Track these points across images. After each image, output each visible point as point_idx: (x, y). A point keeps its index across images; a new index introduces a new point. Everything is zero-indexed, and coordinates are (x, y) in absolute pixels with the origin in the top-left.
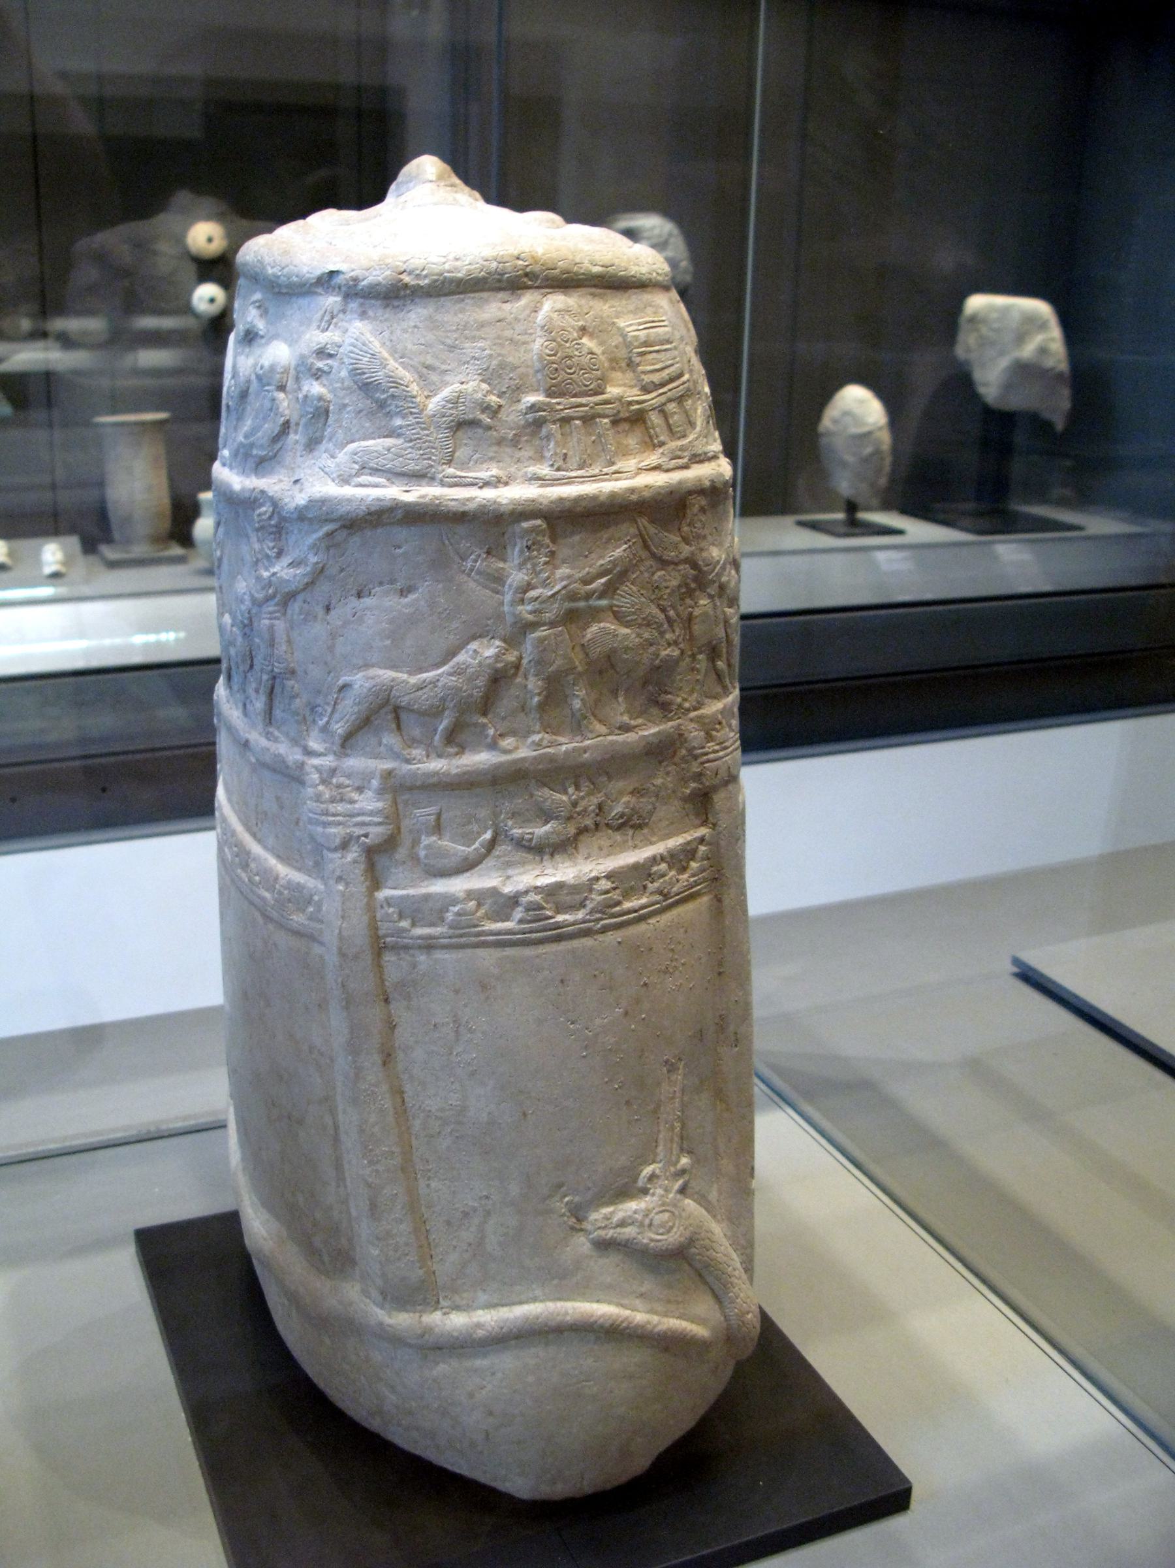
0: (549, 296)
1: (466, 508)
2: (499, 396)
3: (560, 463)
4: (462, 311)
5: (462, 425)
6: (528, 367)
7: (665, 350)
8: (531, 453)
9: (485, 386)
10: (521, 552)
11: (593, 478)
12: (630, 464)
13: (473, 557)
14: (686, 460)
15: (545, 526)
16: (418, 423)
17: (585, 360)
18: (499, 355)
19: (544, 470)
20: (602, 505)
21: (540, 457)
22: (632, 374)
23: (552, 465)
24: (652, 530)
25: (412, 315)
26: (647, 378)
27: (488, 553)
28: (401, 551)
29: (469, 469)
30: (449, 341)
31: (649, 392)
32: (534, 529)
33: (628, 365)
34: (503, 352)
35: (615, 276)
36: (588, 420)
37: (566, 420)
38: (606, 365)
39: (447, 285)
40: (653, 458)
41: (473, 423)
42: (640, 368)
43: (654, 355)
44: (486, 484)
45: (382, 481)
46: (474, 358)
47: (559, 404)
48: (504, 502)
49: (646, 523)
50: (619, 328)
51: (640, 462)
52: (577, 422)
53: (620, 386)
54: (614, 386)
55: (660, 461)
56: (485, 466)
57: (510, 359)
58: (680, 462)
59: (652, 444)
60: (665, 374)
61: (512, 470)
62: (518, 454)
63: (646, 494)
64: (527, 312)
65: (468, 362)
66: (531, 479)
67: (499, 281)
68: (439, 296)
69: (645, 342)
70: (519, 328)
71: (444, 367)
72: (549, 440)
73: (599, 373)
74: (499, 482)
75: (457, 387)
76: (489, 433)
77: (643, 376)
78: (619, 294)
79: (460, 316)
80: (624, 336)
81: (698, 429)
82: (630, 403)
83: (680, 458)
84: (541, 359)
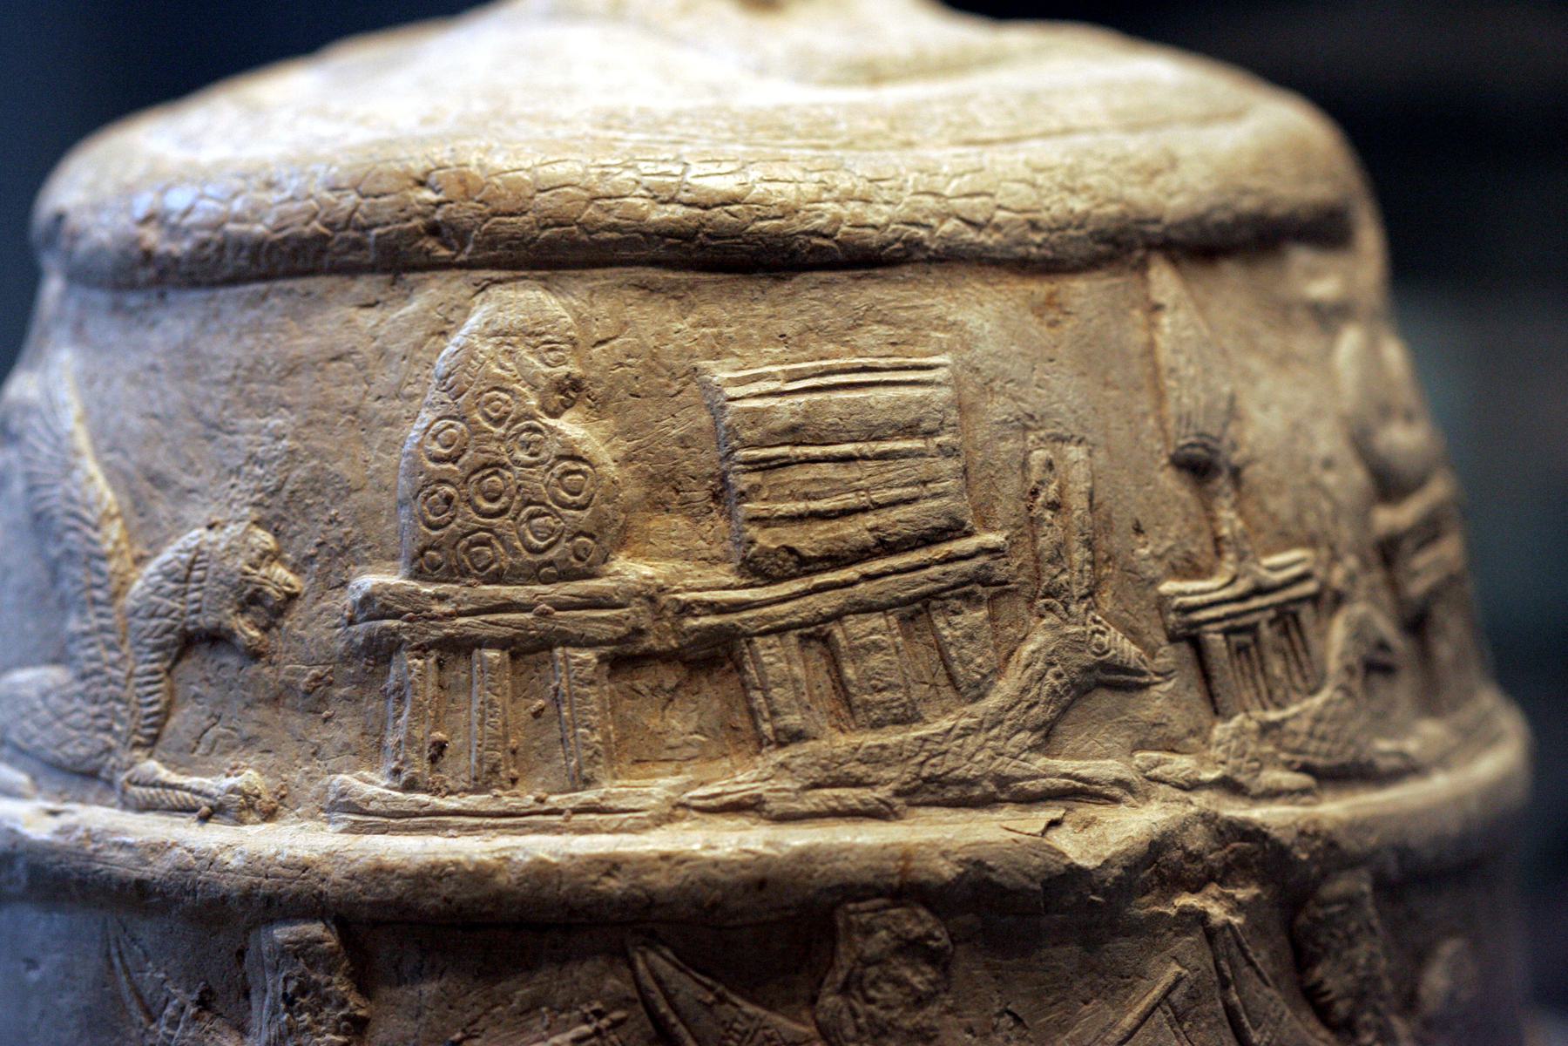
0: (495, 291)
1: (146, 872)
2: (295, 569)
3: (420, 767)
4: (257, 328)
5: (193, 642)
6: (383, 488)
7: (883, 456)
8: (352, 735)
9: (264, 539)
10: (274, 1012)
11: (513, 820)
12: (659, 787)
13: (169, 1011)
14: (882, 793)
15: (332, 941)
16: (103, 629)
17: (539, 481)
18: (314, 453)
19: (373, 785)
20: (499, 897)
21: (369, 750)
22: (721, 523)
23: (397, 772)
24: (688, 988)
25: (155, 338)
26: (765, 539)
27: (204, 1003)
28: (34, 976)
29: (188, 767)
30: (209, 411)
31: (773, 580)
32: (301, 949)
33: (715, 497)
34: (327, 446)
35: (737, 233)
36: (527, 650)
37: (458, 647)
38: (632, 492)
39: (229, 254)
40: (743, 779)
41: (217, 638)
42: (754, 507)
43: (827, 470)
44: (214, 812)
45: (21, 778)
46: (252, 459)
47: (442, 598)
48: (234, 863)
49: (666, 969)
50: (705, 386)
51: (690, 785)
52: (492, 654)
53: (668, 556)
54: (646, 556)
55: (761, 789)
56: (229, 760)
57: (340, 466)
58: (851, 796)
59: (750, 732)
60: (856, 530)
61: (296, 777)
62: (319, 734)
63: (660, 880)
64: (419, 334)
65: (237, 471)
66: (334, 807)
67: (357, 245)
68: (214, 284)
69: (793, 429)
70: (386, 378)
71: (187, 480)
72: (401, 699)
73: (584, 515)
74: (251, 807)
75: (195, 536)
76: (255, 668)
77: (753, 531)
78: (749, 287)
79: (249, 341)
80: (717, 411)
81: (992, 702)
82: (686, 609)
83: (858, 783)
84: (415, 469)
